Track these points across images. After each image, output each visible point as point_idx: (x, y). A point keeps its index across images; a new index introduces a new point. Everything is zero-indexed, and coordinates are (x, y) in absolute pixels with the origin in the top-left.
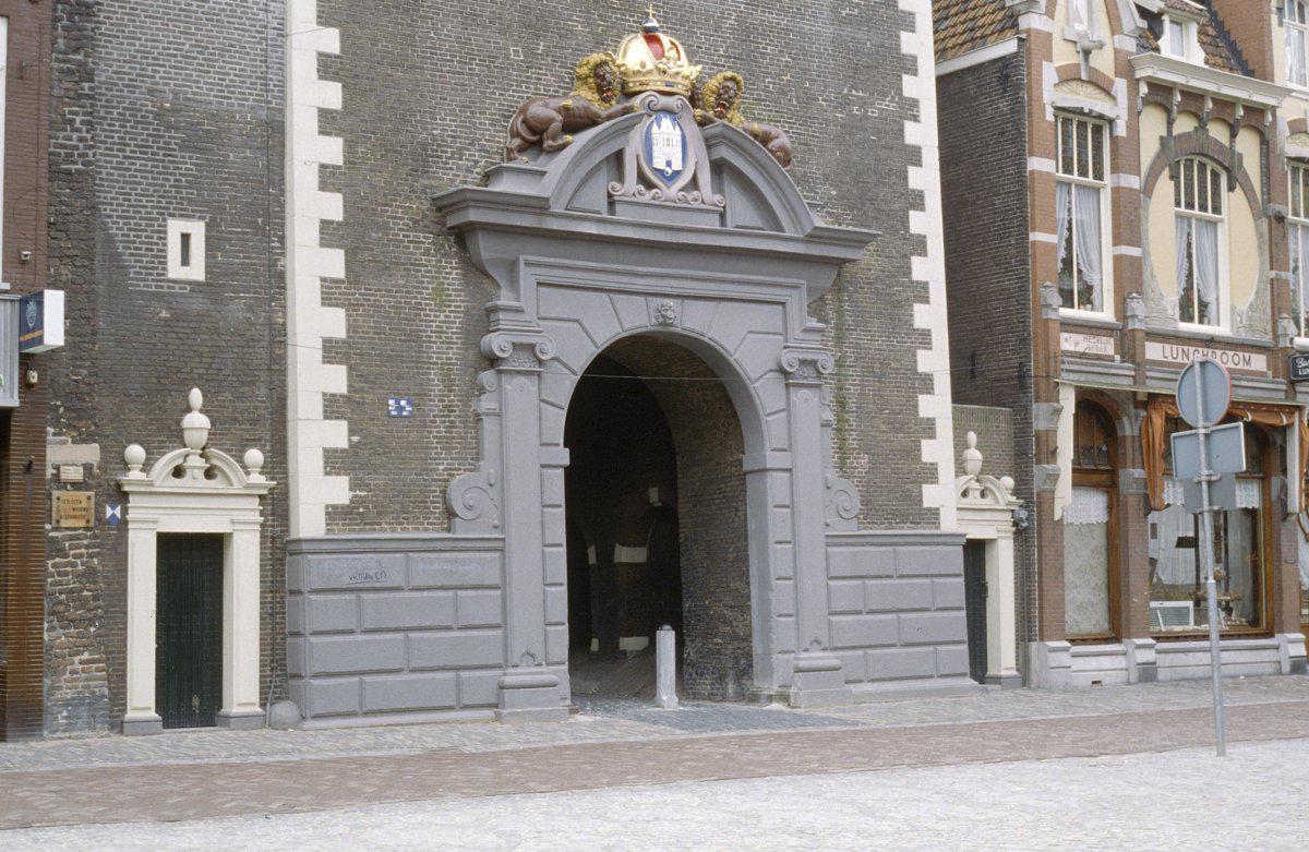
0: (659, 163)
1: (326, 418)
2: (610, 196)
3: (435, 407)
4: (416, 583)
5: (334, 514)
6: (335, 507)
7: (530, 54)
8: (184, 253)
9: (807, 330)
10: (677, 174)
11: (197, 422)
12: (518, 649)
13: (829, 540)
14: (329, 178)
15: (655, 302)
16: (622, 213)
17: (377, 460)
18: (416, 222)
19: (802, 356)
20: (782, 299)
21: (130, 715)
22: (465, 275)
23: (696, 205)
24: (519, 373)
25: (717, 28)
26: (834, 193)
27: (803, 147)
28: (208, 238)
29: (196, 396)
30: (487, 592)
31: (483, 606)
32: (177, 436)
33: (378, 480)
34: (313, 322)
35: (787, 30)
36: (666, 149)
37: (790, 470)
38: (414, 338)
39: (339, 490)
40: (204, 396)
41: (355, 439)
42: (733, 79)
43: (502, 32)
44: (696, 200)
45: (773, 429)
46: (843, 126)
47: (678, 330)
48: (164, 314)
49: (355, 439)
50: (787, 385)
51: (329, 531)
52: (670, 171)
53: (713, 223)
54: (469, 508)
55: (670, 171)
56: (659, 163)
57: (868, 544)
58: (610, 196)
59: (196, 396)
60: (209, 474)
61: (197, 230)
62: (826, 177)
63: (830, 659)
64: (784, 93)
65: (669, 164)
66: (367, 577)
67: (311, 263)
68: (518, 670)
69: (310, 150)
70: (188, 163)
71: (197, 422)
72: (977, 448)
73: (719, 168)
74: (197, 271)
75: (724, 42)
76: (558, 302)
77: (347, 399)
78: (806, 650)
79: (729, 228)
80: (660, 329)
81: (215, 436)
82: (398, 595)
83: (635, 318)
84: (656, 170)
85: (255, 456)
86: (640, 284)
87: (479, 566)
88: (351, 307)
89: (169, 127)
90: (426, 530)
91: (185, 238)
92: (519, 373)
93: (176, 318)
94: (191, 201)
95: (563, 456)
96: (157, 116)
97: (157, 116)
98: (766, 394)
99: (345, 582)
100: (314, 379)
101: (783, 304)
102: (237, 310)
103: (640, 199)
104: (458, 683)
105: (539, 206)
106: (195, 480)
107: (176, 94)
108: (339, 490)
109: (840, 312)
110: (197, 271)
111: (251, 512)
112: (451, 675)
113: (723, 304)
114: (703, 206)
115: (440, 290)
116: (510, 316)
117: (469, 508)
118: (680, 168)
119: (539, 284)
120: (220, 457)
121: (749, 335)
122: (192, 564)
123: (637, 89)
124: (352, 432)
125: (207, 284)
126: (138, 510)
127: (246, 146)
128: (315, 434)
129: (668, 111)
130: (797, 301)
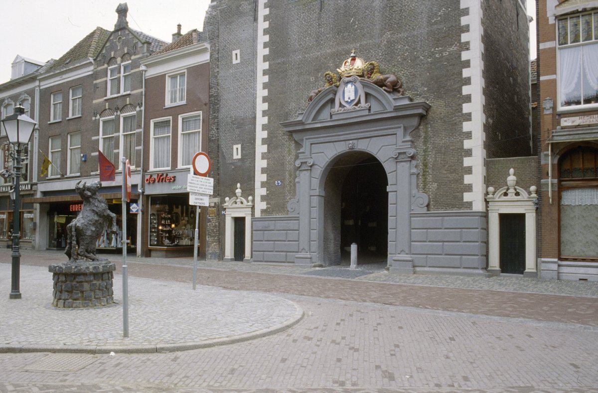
0: (346, 99)
1: (262, 187)
2: (331, 113)
3: (287, 182)
4: (278, 229)
5: (263, 211)
6: (263, 210)
7: (317, 78)
8: (237, 152)
9: (403, 142)
10: (353, 101)
11: (238, 191)
12: (301, 248)
13: (411, 215)
14: (264, 127)
15: (348, 142)
16: (334, 118)
17: (272, 197)
18: (284, 134)
20: (395, 133)
21: (226, 257)
22: (295, 145)
24: (304, 170)
25: (379, 46)
26: (426, 89)
27: (412, 77)
28: (241, 148)
29: (239, 185)
30: (295, 231)
31: (293, 235)
32: (235, 194)
33: (273, 202)
34: (260, 163)
35: (407, 38)
37: (396, 191)
38: (283, 164)
39: (263, 205)
40: (241, 185)
41: (268, 192)
42: (371, 64)
43: (308, 75)
45: (391, 178)
46: (431, 63)
47: (357, 150)
48: (233, 167)
49: (268, 192)
50: (397, 162)
51: (261, 216)
52: (349, 100)
53: (367, 113)
54: (292, 209)
55: (349, 100)
56: (346, 99)
57: (432, 216)
58: (331, 113)
59: (239, 185)
60: (517, 194)
61: (239, 146)
62: (423, 84)
63: (408, 257)
64: (405, 60)
65: (349, 98)
66: (266, 227)
67: (261, 149)
68: (301, 253)
69: (261, 121)
70: (237, 131)
71: (238, 191)
72: (514, 175)
73: (367, 95)
74: (239, 157)
76: (316, 148)
77: (266, 182)
78: (399, 254)
79: (372, 113)
80: (350, 150)
81: (517, 183)
82: (273, 232)
83: (341, 148)
85: (250, 198)
86: (342, 138)
87: (292, 224)
88: (268, 159)
89: (234, 124)
90: (284, 215)
91: (237, 149)
92: (304, 170)
93: (235, 168)
94: (238, 140)
95: (389, 189)
96: (232, 123)
97: (232, 123)
98: (388, 167)
99: (261, 228)
100: (260, 178)
102: (247, 164)
103: (340, 112)
104: (286, 255)
105: (301, 123)
106: (239, 205)
107: (235, 116)
108: (263, 205)
109: (426, 132)
110: (239, 157)
111: (249, 211)
112: (285, 253)
113: (373, 139)
115: (290, 150)
116: (302, 155)
117: (292, 209)
118: (354, 98)
119: (311, 144)
120: (519, 189)
121: (383, 148)
122: (239, 222)
124: (267, 191)
125: (241, 159)
126: (228, 212)
127: (249, 124)
128: (260, 191)
130: (400, 132)
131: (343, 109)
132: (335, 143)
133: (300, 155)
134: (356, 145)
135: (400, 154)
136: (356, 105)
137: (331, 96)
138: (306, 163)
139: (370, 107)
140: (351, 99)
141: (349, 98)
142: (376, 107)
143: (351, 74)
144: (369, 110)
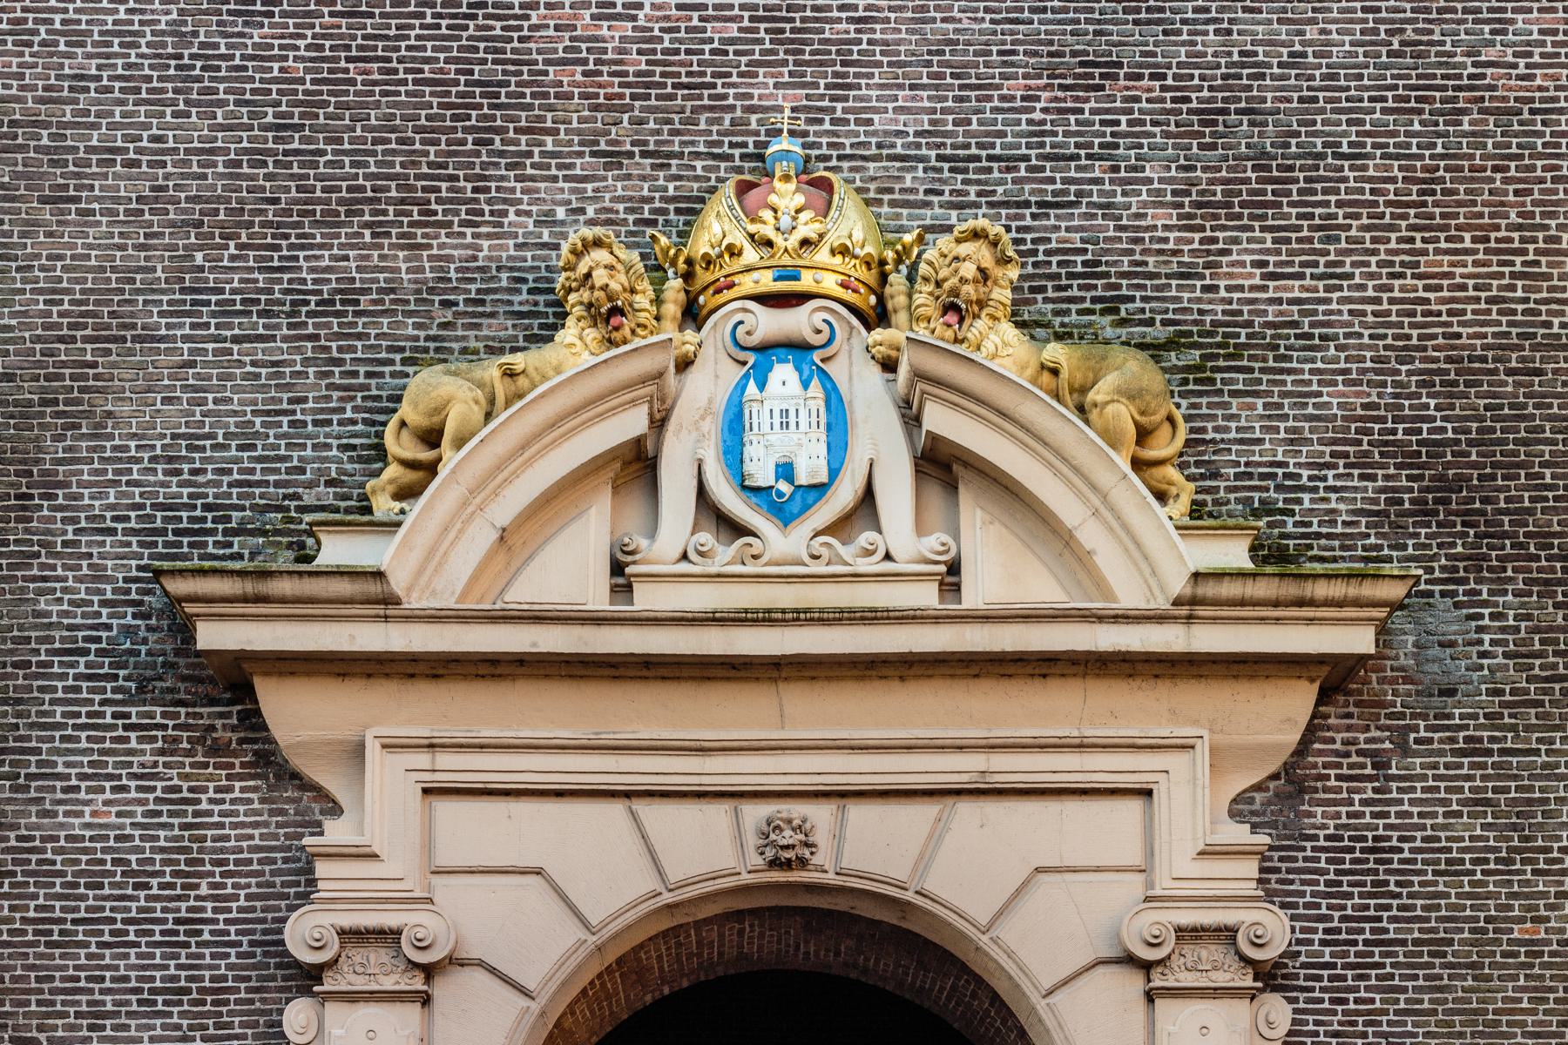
10: (820, 489)
16: (647, 598)
19: (1188, 918)
23: (864, 565)
36: (777, 437)
44: (869, 553)
50: (1150, 997)
53: (926, 596)
65: (786, 471)
75: (1008, 170)
84: (756, 490)
101: (1148, 793)
114: (888, 567)
118: (823, 477)
123: (710, 306)
129: (797, 347)
131: (725, 555)
132: (643, 808)
133: (322, 869)
134: (821, 837)
135: (1188, 934)
136: (841, 527)
137: (633, 423)
138: (388, 937)
139: (954, 568)
140: (803, 478)
141: (786, 471)
142: (1001, 568)
143: (807, 282)
144: (951, 576)
